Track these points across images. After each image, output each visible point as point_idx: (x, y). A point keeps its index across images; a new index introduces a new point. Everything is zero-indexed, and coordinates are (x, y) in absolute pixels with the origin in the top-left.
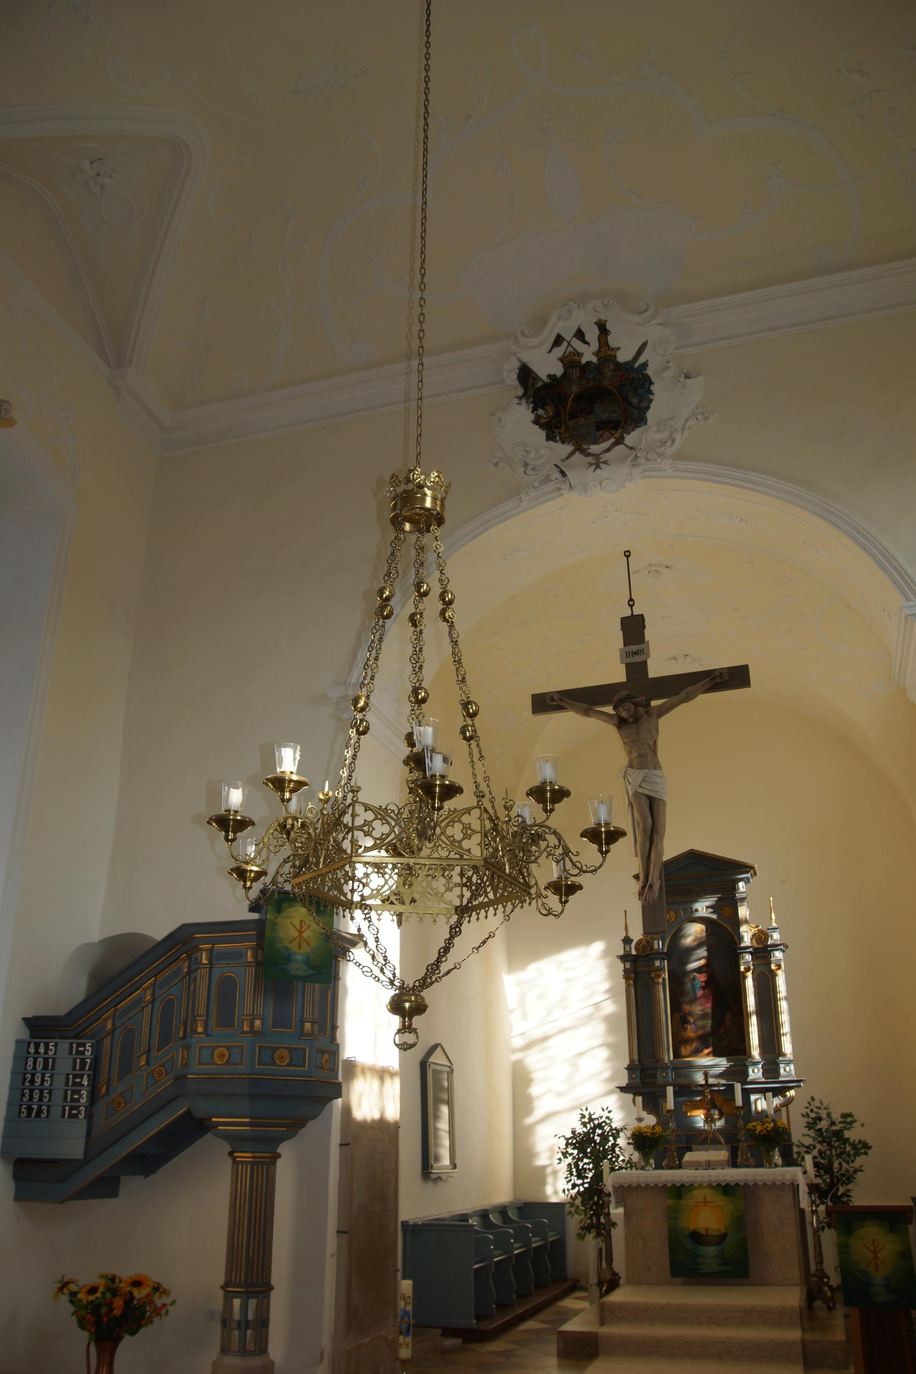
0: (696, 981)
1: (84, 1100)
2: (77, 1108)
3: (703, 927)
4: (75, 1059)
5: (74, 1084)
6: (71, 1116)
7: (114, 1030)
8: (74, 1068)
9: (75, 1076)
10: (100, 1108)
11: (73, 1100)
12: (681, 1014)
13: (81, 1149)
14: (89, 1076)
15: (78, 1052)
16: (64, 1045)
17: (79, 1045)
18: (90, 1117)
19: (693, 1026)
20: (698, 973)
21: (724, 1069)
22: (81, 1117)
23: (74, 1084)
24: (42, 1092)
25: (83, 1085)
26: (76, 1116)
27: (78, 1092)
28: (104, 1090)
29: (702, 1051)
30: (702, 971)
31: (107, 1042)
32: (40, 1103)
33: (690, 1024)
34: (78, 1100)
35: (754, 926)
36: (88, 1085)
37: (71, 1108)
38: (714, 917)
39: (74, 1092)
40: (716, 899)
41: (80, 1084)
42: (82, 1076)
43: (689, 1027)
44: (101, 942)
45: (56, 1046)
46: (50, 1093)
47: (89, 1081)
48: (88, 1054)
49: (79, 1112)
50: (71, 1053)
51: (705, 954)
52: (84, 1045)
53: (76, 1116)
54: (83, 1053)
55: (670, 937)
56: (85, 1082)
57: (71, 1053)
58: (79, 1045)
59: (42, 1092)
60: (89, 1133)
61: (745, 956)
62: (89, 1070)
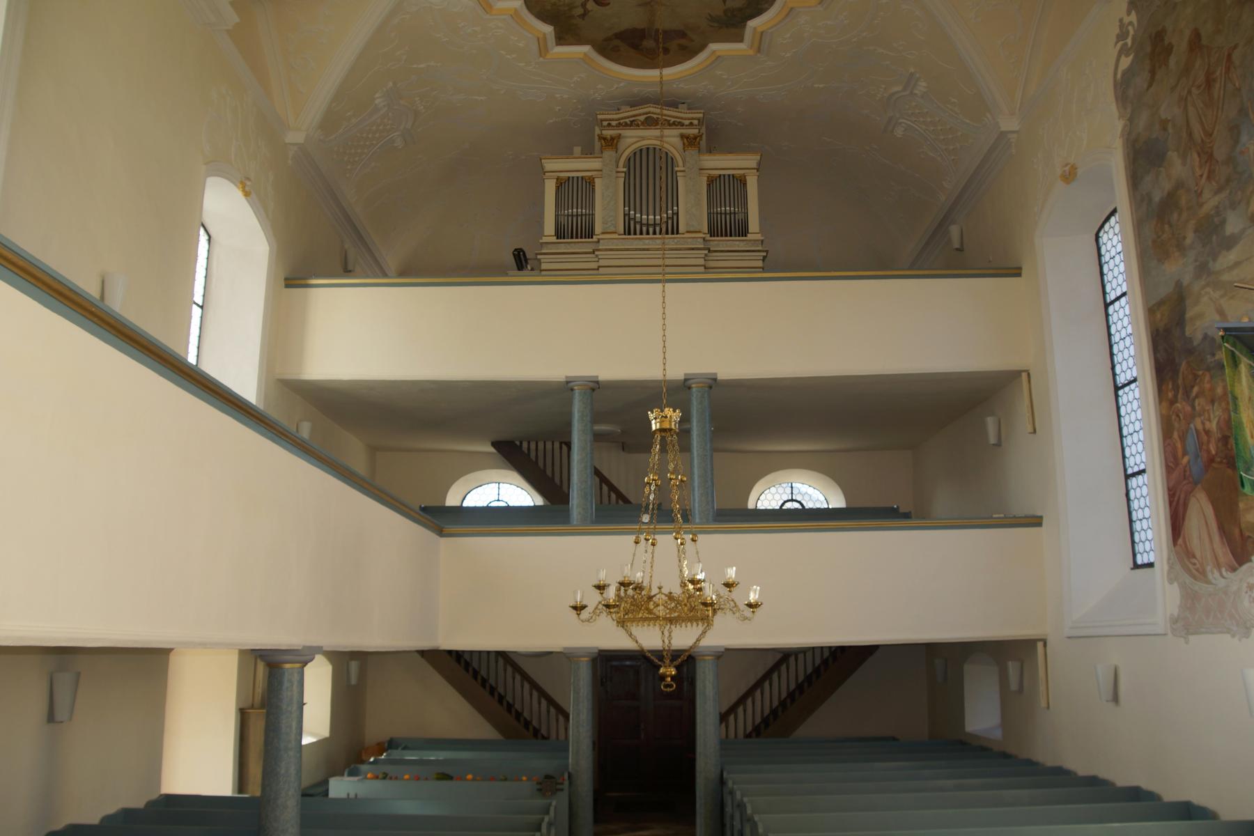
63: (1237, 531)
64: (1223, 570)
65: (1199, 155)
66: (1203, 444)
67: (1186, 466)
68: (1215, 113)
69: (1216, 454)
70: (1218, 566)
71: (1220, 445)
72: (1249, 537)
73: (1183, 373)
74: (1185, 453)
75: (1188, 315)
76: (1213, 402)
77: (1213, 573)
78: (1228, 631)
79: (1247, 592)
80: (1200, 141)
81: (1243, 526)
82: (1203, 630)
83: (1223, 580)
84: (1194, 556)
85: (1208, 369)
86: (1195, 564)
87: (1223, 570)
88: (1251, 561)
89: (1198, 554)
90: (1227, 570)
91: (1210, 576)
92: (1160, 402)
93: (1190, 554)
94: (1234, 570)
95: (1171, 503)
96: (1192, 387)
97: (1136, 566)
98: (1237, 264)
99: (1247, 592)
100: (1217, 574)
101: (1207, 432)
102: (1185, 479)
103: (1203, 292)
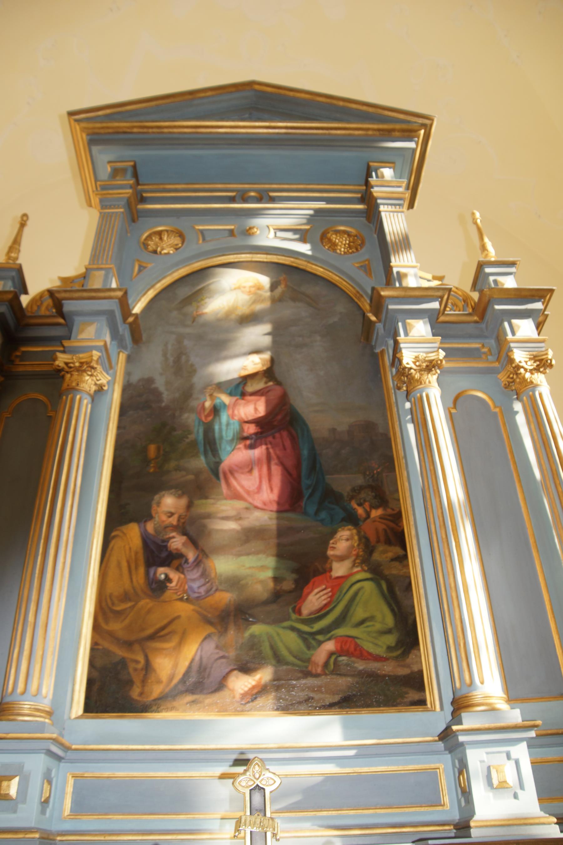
0: (224, 417)
3: (265, 280)
12: (150, 527)
19: (195, 574)
20: (231, 394)
21: (331, 769)
29: (221, 686)
30: (250, 388)
33: (179, 569)
35: (430, 277)
38: (305, 248)
40: (311, 212)
43: (174, 576)
51: (267, 340)
55: (151, 294)
61: (412, 327)
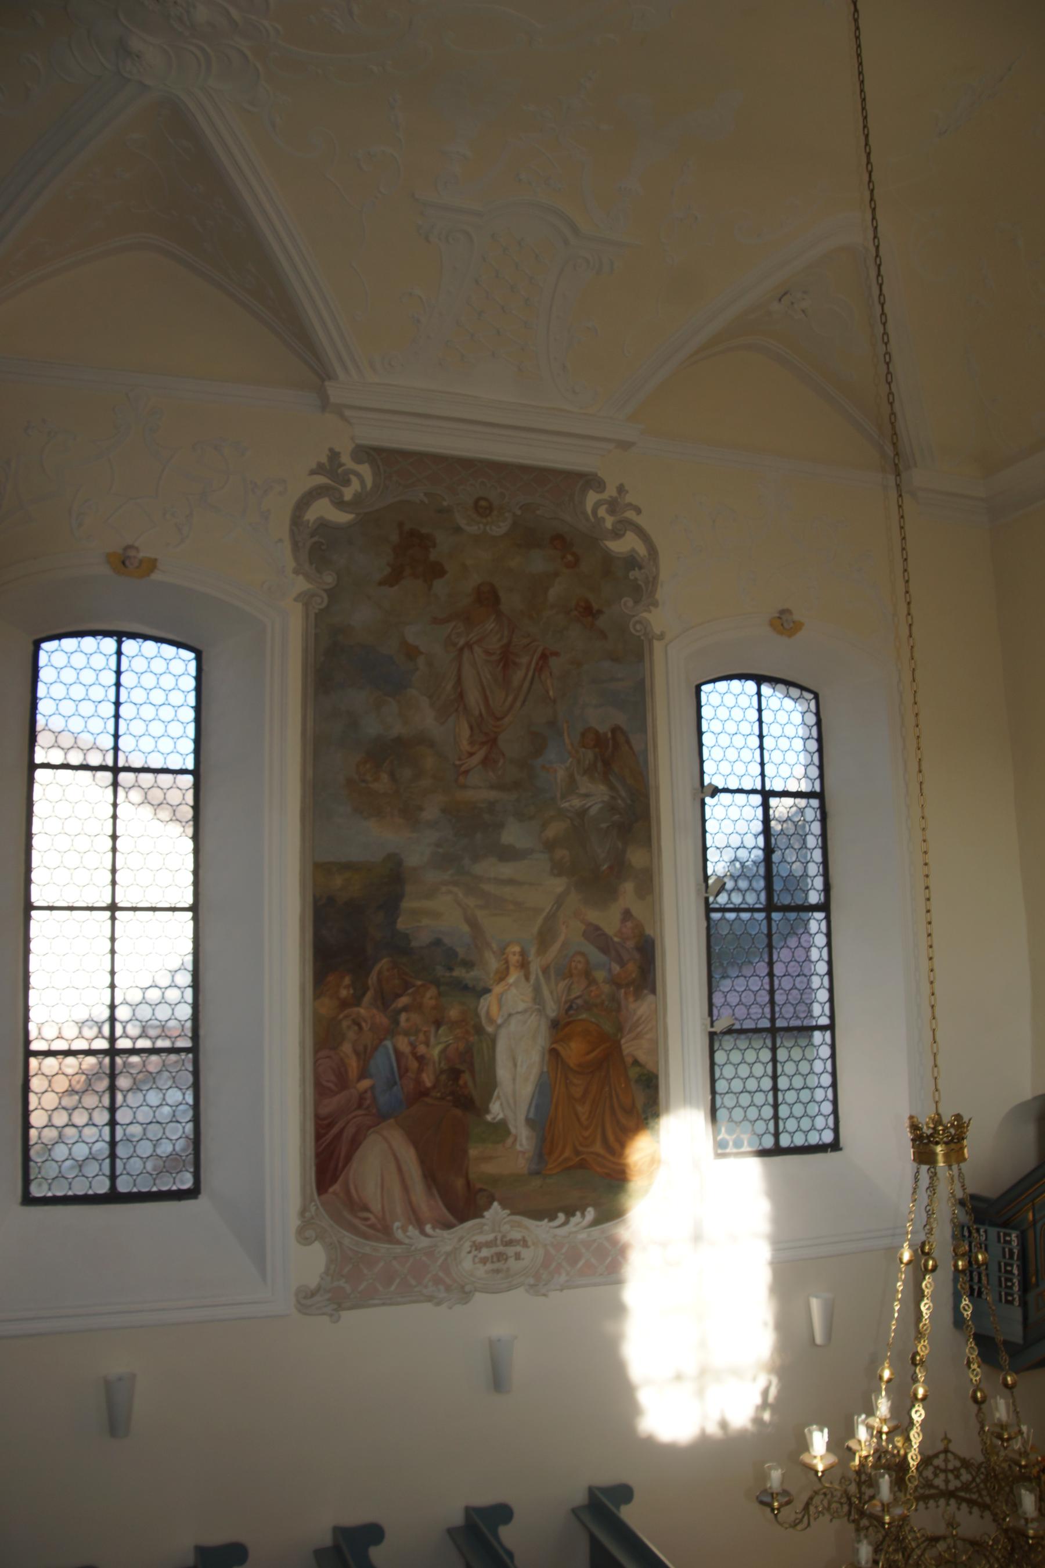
1: (1016, 1288)
2: (1012, 1295)
4: (1004, 1249)
5: (1006, 1271)
6: (1007, 1302)
7: (1035, 1222)
8: (1004, 1256)
9: (1006, 1265)
10: (1031, 1297)
11: (1007, 1287)
13: (1018, 1329)
14: (1018, 1266)
15: (1006, 1242)
16: (993, 1231)
17: (1005, 1235)
18: (1024, 1304)
22: (1017, 1303)
23: (1006, 1271)
24: (979, 1274)
25: (1014, 1274)
26: (1011, 1302)
27: (1011, 1280)
28: (1034, 1280)
31: (1030, 1234)
32: (980, 1285)
34: (1011, 1288)
36: (1019, 1275)
37: (1007, 1294)
39: (1007, 1280)
41: (1011, 1272)
42: (1011, 1265)
44: (1035, 1099)
45: (986, 1232)
46: (987, 1275)
47: (1018, 1270)
48: (1015, 1243)
49: (1014, 1299)
50: (999, 1241)
52: (1010, 1235)
53: (1011, 1302)
54: (1009, 1242)
56: (1015, 1271)
57: (999, 1241)
58: (1005, 1235)
59: (979, 1274)
60: (1025, 1318)
62: (1018, 1259)
63: (460, 1183)
64: (428, 1228)
65: (471, 728)
66: (407, 1070)
67: (366, 1092)
68: (510, 699)
69: (434, 1087)
70: (420, 1225)
71: (443, 1077)
72: (481, 1190)
73: (380, 973)
74: (363, 1075)
75: (406, 904)
76: (438, 1024)
77: (405, 1231)
78: (430, 1299)
79: (469, 1252)
80: (477, 713)
81: (472, 1176)
82: (376, 1302)
83: (423, 1238)
84: (366, 1208)
85: (437, 983)
86: (366, 1219)
87: (428, 1228)
88: (482, 1217)
89: (376, 1206)
90: (434, 1228)
91: (399, 1234)
92: (318, 993)
93: (356, 1206)
94: (448, 1226)
95: (318, 1137)
96: (398, 996)
97: (28, 1200)
98: (511, 882)
99: (469, 1252)
100: (412, 1231)
101: (421, 1059)
102: (360, 1106)
103: (444, 889)
